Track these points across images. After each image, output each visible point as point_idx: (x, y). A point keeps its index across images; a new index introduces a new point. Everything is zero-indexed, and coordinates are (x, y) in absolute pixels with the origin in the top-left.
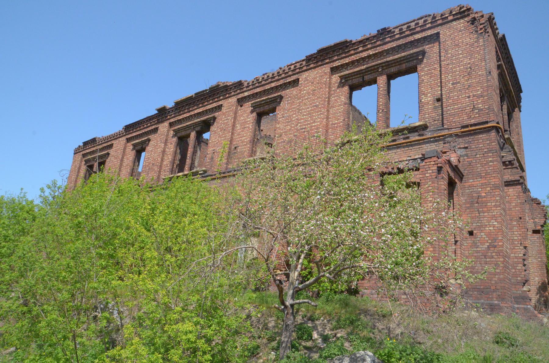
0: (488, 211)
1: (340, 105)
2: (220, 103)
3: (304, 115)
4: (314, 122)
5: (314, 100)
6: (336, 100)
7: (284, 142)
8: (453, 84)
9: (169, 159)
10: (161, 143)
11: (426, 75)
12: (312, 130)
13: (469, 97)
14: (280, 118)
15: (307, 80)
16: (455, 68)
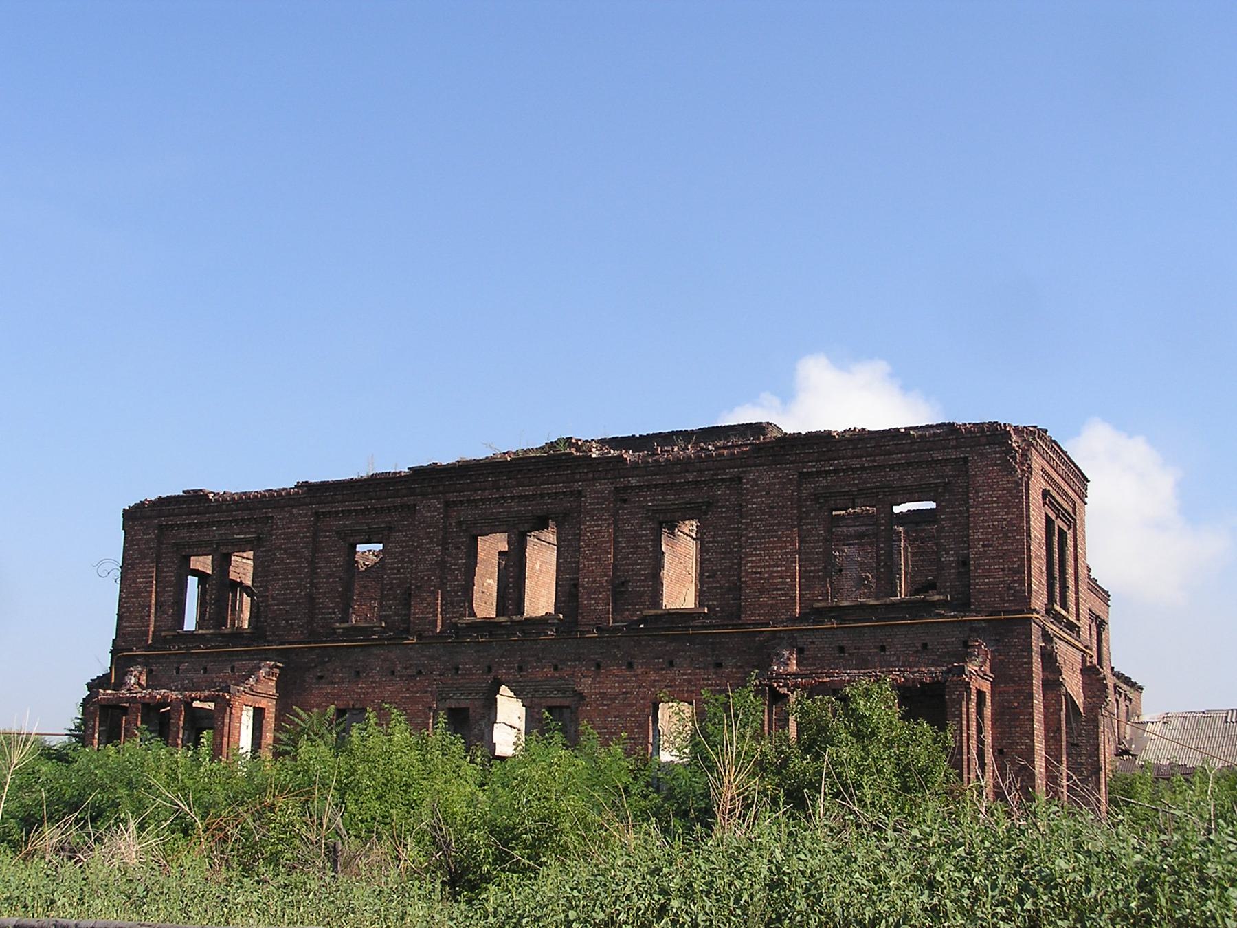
0: (1020, 726)
1: (818, 541)
2: (577, 486)
3: (756, 549)
4: (776, 565)
5: (773, 525)
6: (809, 530)
7: (721, 588)
8: (984, 546)
9: (457, 580)
10: (431, 542)
11: (950, 519)
12: (771, 577)
13: (1003, 570)
14: (709, 542)
15: (758, 485)
16: (986, 521)
